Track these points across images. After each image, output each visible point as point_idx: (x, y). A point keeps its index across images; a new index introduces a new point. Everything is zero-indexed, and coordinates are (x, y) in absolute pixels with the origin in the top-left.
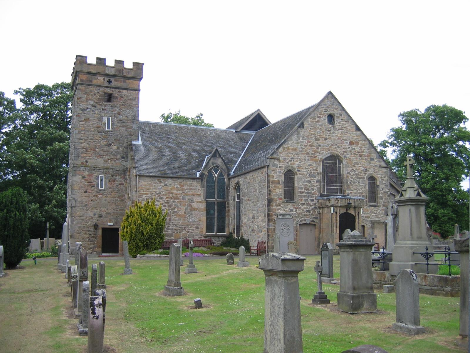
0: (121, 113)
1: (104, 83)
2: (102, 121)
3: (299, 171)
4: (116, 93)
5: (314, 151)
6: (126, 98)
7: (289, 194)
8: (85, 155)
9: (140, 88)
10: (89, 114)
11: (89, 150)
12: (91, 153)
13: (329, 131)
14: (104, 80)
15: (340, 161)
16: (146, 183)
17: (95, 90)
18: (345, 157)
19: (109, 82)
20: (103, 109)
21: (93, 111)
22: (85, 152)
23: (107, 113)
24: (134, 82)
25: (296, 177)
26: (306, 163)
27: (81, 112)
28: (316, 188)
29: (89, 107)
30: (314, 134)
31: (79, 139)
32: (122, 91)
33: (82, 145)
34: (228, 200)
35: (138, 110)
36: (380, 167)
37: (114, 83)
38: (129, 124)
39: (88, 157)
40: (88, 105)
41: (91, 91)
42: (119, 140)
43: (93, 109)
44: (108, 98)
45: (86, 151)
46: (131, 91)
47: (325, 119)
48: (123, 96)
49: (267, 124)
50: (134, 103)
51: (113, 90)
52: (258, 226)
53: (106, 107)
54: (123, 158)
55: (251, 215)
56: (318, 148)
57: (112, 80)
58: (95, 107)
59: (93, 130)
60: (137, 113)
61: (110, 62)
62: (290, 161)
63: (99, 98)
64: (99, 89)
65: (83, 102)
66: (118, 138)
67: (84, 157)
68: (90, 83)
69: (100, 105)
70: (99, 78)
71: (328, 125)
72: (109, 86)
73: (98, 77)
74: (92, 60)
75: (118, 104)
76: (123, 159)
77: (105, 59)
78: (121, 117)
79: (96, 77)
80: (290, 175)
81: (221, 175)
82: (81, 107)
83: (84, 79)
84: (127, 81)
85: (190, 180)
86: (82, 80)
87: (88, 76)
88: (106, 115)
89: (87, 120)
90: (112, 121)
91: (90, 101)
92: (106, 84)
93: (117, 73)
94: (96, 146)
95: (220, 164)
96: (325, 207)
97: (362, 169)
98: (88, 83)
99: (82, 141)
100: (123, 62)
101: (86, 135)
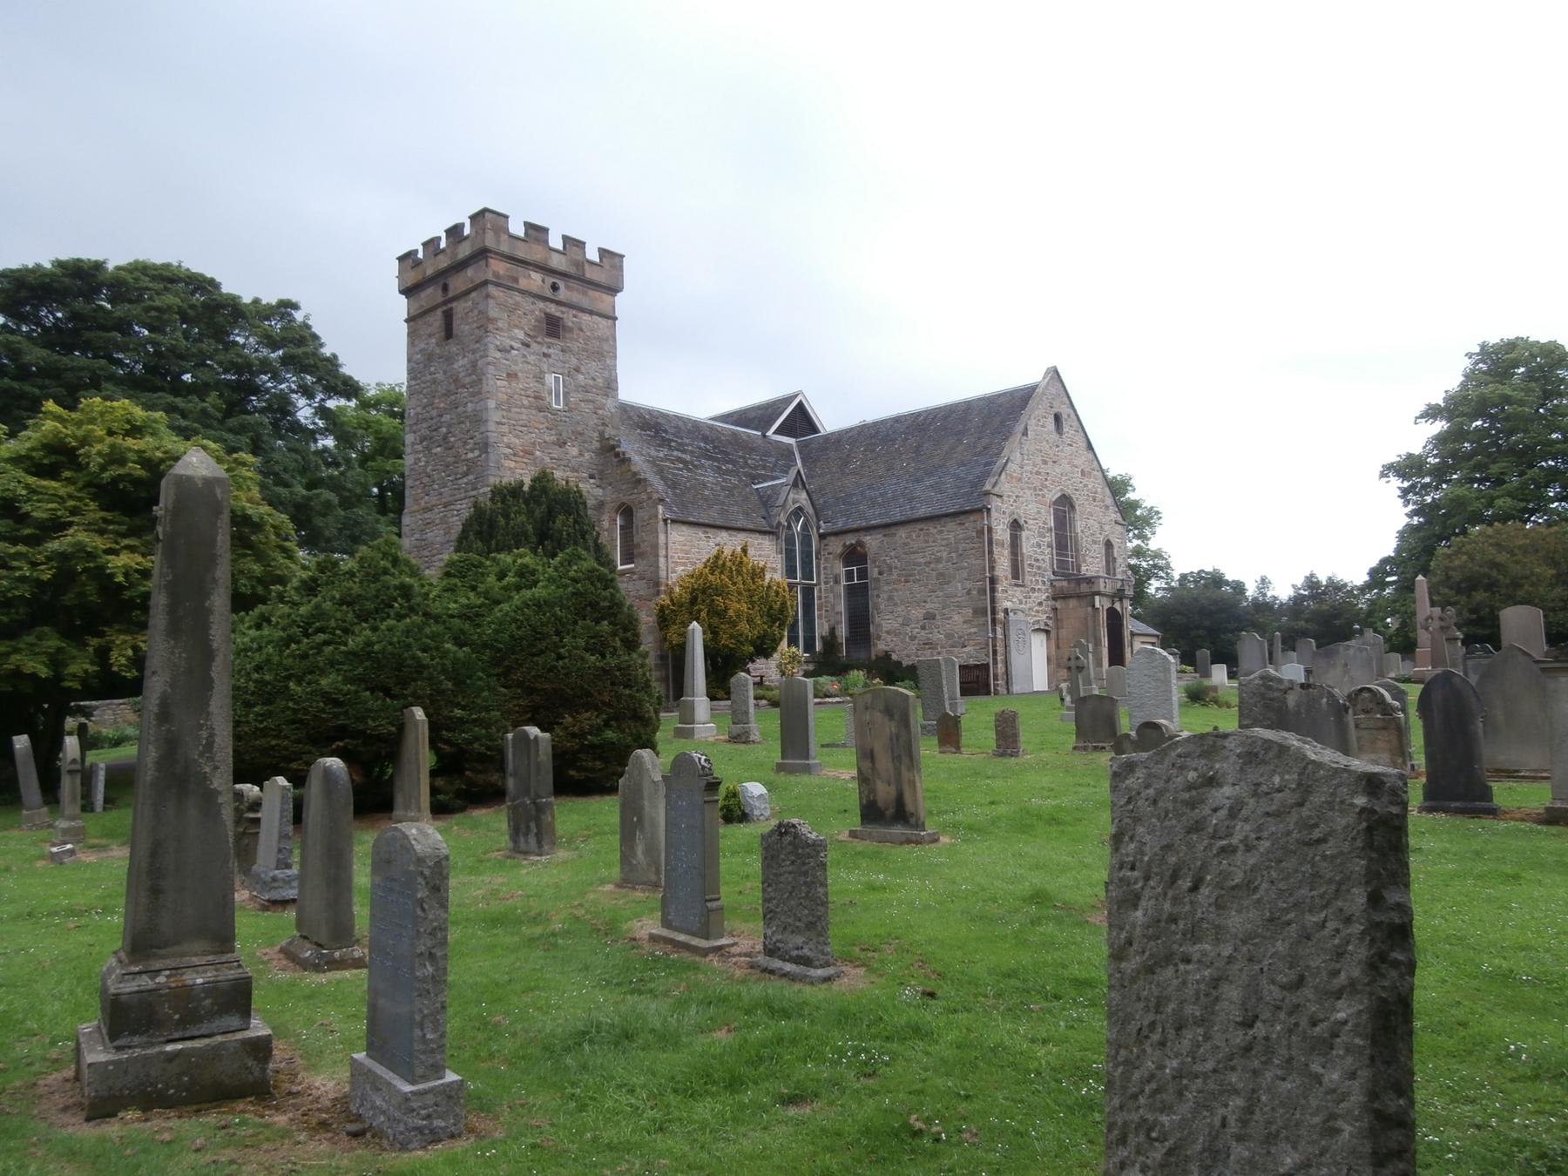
0: (583, 369)
1: (543, 288)
2: (543, 384)
3: (1026, 522)
4: (569, 317)
5: (1042, 485)
6: (588, 334)
7: (1016, 572)
8: (512, 464)
9: (617, 314)
10: (516, 363)
11: (521, 454)
12: (525, 460)
13: (1057, 446)
14: (543, 281)
15: (1072, 507)
16: (682, 539)
17: (526, 304)
18: (1077, 499)
19: (555, 288)
20: (545, 355)
21: (524, 356)
22: (512, 457)
23: (553, 366)
24: (605, 297)
25: (1024, 534)
26: (1033, 508)
27: (498, 355)
28: (1047, 558)
29: (516, 345)
30: (1041, 451)
31: (498, 423)
32: (580, 314)
33: (505, 439)
34: (818, 584)
35: (615, 366)
36: (1116, 523)
37: (563, 294)
38: (599, 398)
39: (521, 471)
40: (512, 338)
41: (517, 304)
42: (580, 434)
43: (524, 351)
44: (553, 327)
45: (515, 455)
46: (599, 319)
47: (1051, 419)
48: (584, 327)
49: (815, 430)
50: (606, 347)
51: (564, 309)
52: (949, 636)
53: (551, 351)
54: (591, 477)
55: (917, 613)
56: (1046, 480)
57: (561, 284)
58: (528, 346)
59: (525, 402)
60: (613, 374)
61: (556, 242)
62: (1015, 501)
63: (534, 326)
64: (533, 303)
65: (502, 330)
66: (579, 429)
67: (510, 469)
68: (515, 286)
69: (539, 343)
70: (533, 274)
71: (1055, 436)
72: (552, 297)
73: (531, 273)
74: (517, 229)
75: (575, 346)
76: (592, 481)
77: (545, 230)
78: (581, 377)
79: (527, 272)
80: (1016, 526)
81: (805, 527)
82: (498, 343)
83: (501, 272)
84: (593, 294)
85: (757, 535)
86: (496, 275)
87: (508, 265)
88: (552, 369)
89: (512, 376)
90: (564, 386)
91: (516, 331)
92: (548, 293)
93: (572, 270)
94: (534, 444)
95: (804, 502)
96: (1071, 597)
97: (1097, 525)
98: (509, 285)
99: (505, 429)
100: (584, 243)
101: (510, 415)
